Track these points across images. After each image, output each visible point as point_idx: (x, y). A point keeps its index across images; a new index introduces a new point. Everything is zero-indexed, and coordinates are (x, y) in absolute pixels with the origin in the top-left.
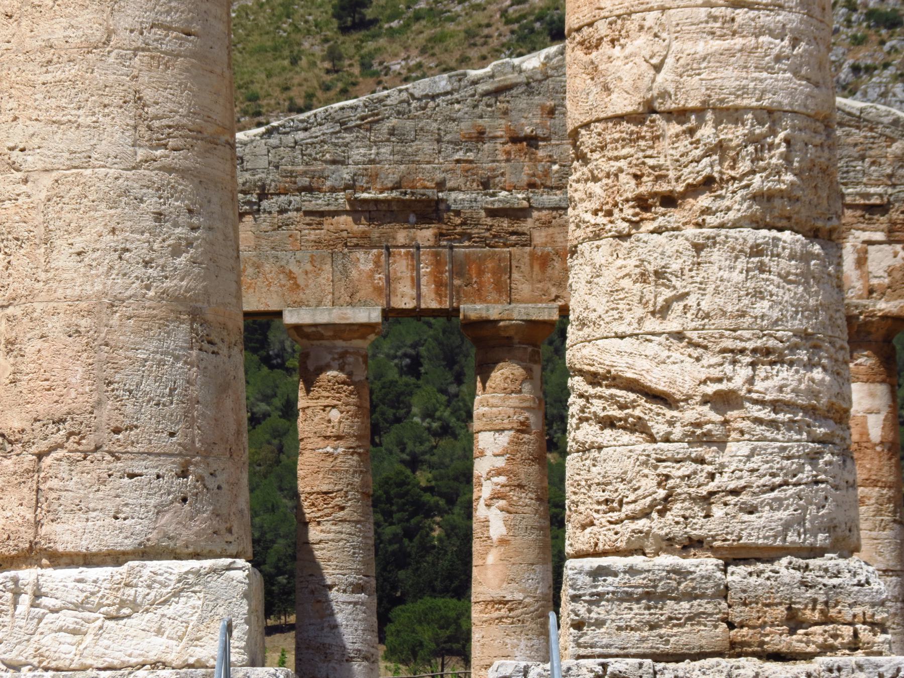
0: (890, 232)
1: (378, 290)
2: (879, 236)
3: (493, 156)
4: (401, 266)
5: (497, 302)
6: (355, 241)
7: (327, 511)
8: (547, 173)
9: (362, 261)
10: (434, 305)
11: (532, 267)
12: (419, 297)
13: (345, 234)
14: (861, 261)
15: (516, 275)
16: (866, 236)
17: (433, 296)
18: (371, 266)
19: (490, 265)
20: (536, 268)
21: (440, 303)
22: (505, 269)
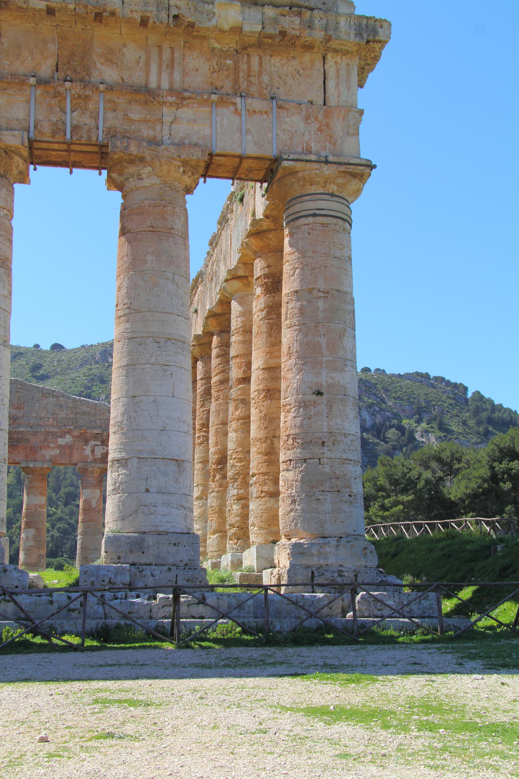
2: (99, 443)
14: (93, 451)
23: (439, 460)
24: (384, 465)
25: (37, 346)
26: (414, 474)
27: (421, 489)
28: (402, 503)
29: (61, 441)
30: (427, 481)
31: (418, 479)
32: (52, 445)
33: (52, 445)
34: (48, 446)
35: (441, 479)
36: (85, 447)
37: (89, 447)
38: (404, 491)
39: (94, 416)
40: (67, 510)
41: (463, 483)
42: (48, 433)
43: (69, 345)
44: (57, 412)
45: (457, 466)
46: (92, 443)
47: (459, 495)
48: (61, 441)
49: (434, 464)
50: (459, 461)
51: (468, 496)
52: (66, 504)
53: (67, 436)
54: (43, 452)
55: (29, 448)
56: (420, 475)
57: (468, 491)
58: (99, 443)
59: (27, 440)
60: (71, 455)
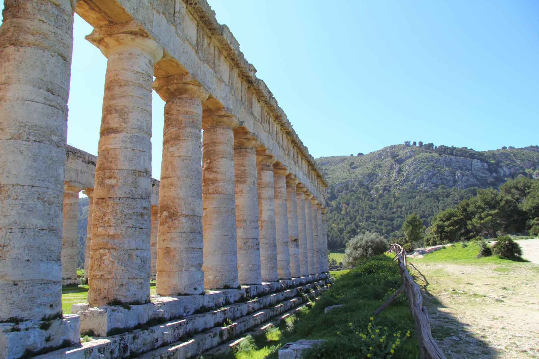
23: (517, 188)
24: (481, 194)
25: (352, 155)
26: (499, 198)
27: (502, 207)
28: (491, 215)
30: (507, 201)
31: (501, 200)
35: (518, 199)
38: (493, 208)
40: (367, 224)
41: (531, 200)
43: (365, 153)
45: (527, 191)
47: (528, 208)
49: (513, 191)
50: (529, 188)
51: (534, 208)
52: (367, 221)
56: (502, 197)
57: (534, 205)
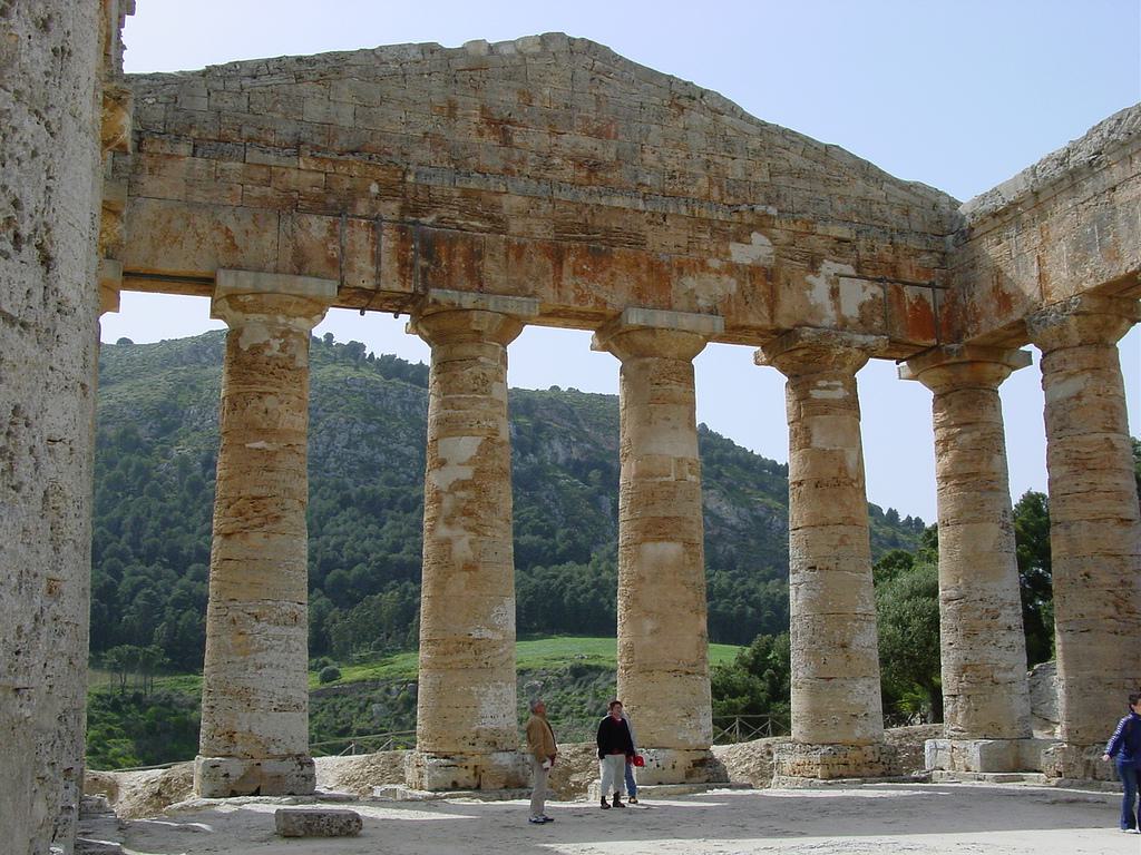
0: (858, 266)
1: (332, 262)
3: (466, 132)
4: (359, 237)
5: (468, 290)
6: (306, 204)
7: (257, 521)
8: (523, 161)
9: (315, 227)
10: (397, 287)
11: (507, 256)
12: (378, 275)
13: (295, 195)
14: (835, 293)
15: (489, 264)
16: (837, 268)
17: (397, 276)
18: (324, 234)
19: (460, 248)
20: (512, 257)
21: (404, 284)
22: (475, 255)
29: (741, 254)
32: (714, 263)
33: (714, 263)
34: (703, 266)
36: (810, 278)
37: (823, 277)
39: (826, 182)
42: (700, 223)
44: (718, 159)
46: (829, 267)
48: (741, 254)
53: (756, 237)
54: (690, 282)
55: (644, 267)
58: (850, 270)
59: (637, 241)
60: (773, 302)
